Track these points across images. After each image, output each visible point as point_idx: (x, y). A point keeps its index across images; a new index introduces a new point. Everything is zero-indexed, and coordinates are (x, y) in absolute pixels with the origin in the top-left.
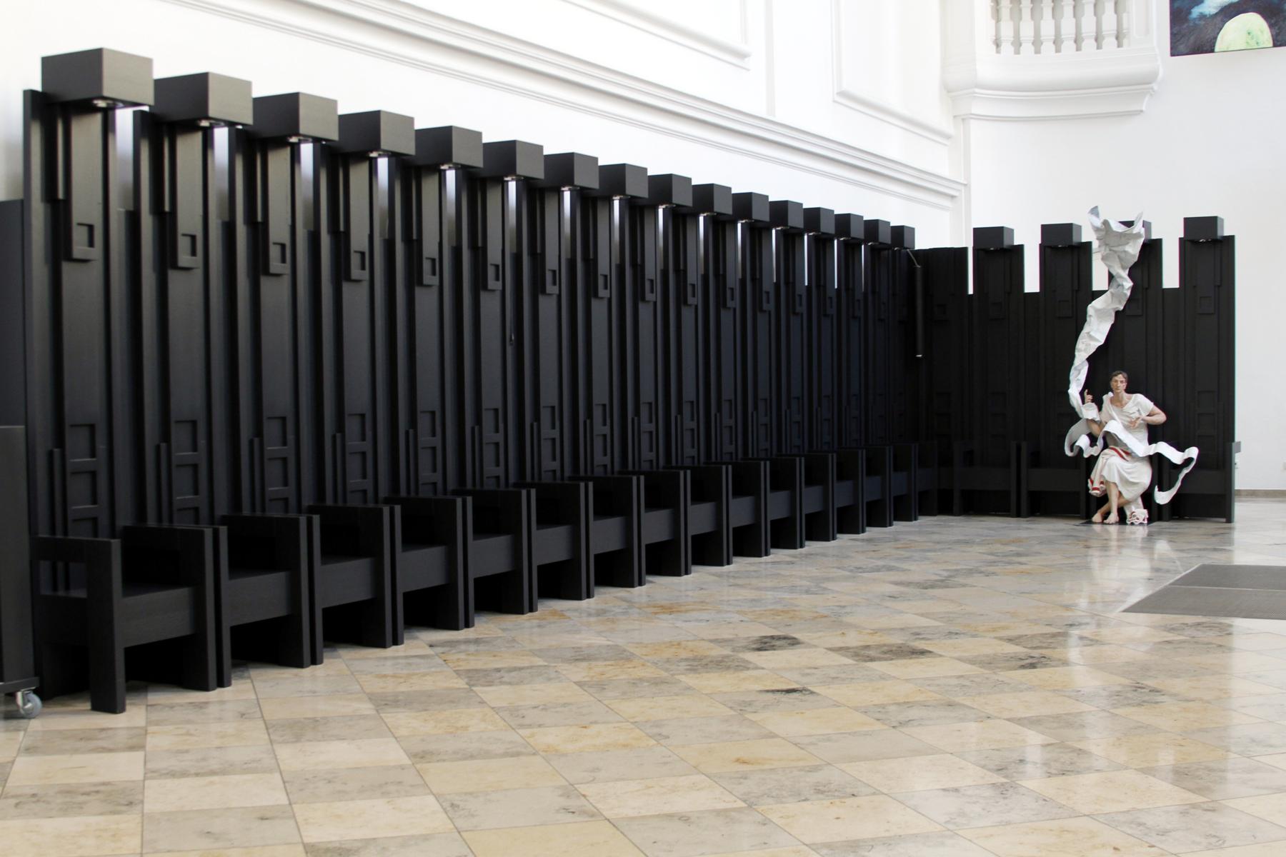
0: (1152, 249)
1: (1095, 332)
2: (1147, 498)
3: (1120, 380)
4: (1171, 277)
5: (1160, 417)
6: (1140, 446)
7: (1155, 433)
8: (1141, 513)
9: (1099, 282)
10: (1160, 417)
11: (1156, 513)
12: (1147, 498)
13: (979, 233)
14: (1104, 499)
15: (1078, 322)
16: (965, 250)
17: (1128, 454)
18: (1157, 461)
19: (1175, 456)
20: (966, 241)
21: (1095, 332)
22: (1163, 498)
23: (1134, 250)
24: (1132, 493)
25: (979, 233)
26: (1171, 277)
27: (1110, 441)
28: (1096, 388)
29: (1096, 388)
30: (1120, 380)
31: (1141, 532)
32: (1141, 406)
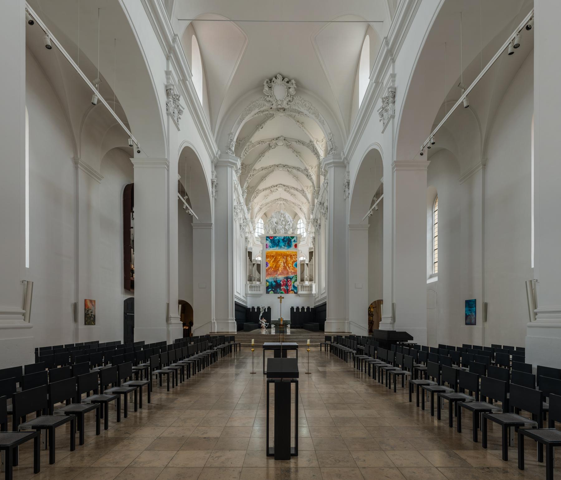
0: (265, 308)
1: (261, 315)
2: (265, 327)
3: (263, 318)
4: (266, 311)
5: (266, 321)
6: (265, 323)
7: (266, 322)
8: (265, 328)
9: (261, 311)
10: (266, 321)
11: (266, 328)
12: (265, 327)
13: (252, 307)
14: (262, 327)
15: (260, 314)
16: (250, 308)
17: (264, 324)
18: (266, 324)
19: (267, 324)
20: (251, 307)
21: (261, 315)
22: (267, 327)
23: (264, 309)
24: (264, 327)
25: (252, 307)
26: (266, 311)
27: (263, 323)
28: (261, 319)
29: (261, 319)
30: (263, 318)
31: (265, 329)
32: (265, 320)
